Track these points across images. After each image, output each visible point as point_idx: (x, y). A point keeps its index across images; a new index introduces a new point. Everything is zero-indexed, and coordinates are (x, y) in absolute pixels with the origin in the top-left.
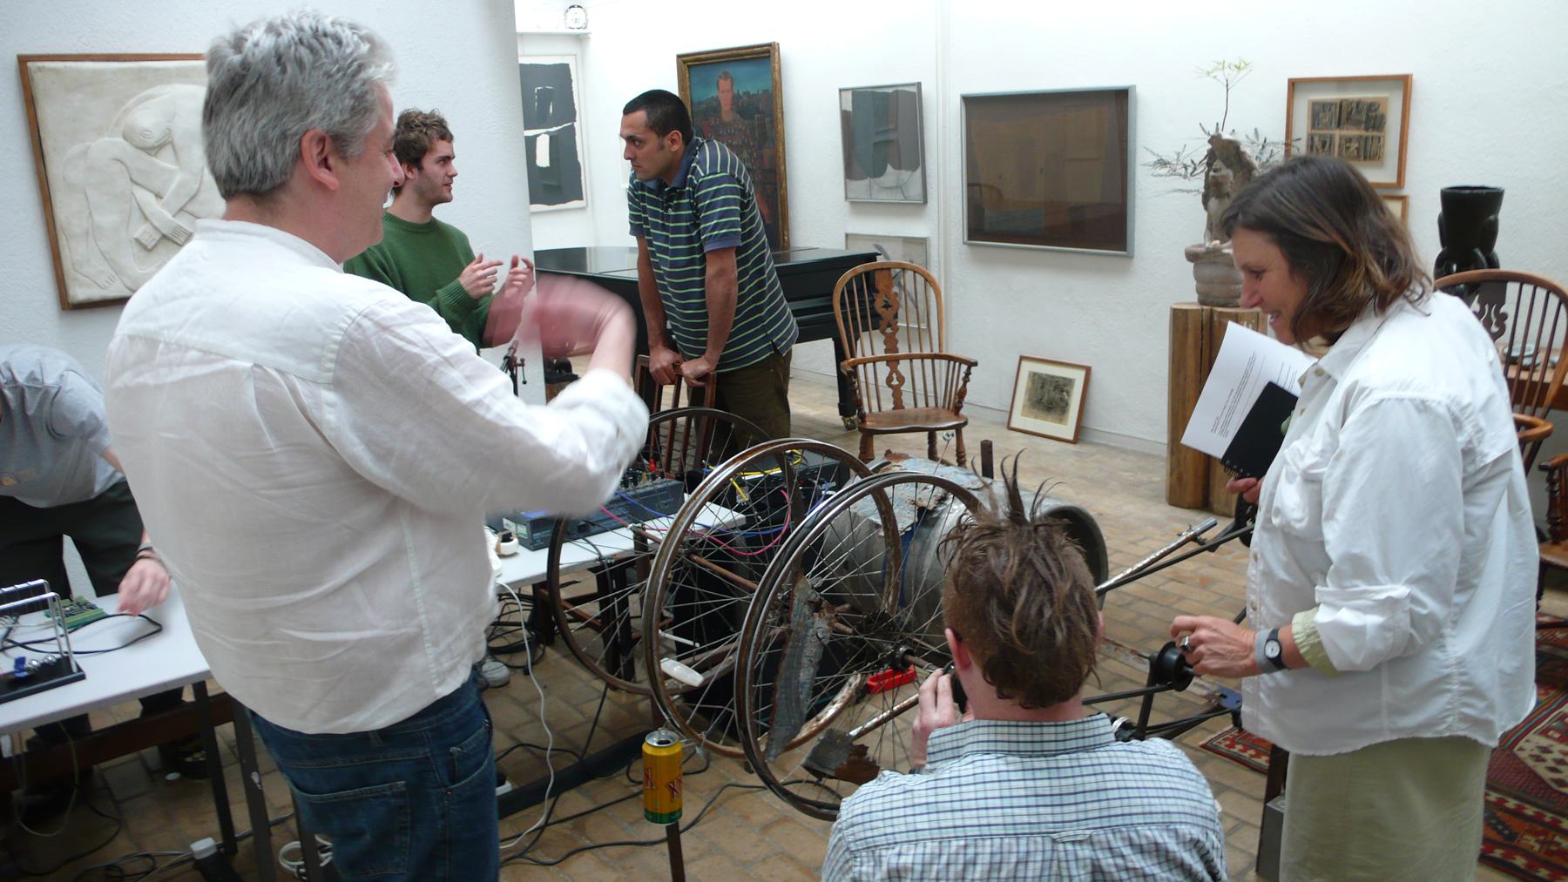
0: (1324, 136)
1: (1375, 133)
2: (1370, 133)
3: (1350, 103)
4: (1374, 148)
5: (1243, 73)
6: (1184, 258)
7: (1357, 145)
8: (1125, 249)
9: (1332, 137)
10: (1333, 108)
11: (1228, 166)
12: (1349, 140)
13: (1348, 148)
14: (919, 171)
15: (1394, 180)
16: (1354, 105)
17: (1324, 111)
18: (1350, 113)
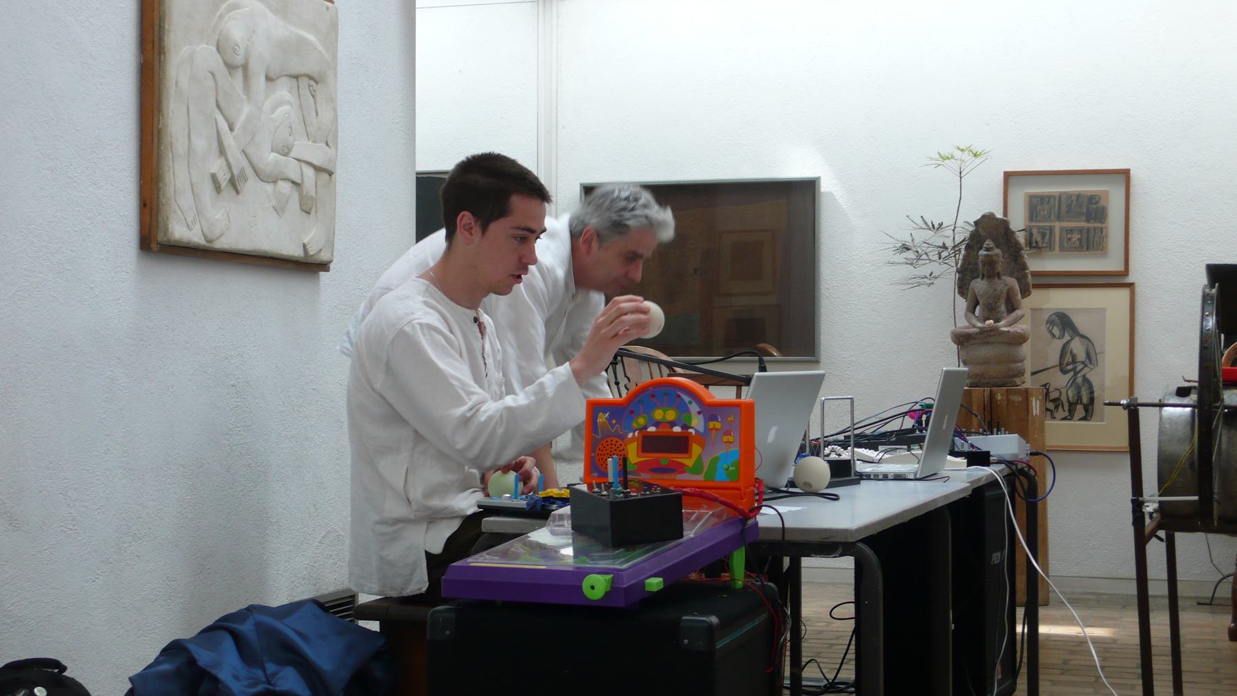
2: (1089, 225)
4: (1096, 239)
5: (978, 160)
6: (950, 340)
7: (1079, 236)
8: (814, 356)
9: (1051, 229)
10: (1052, 200)
11: (998, 246)
12: (1071, 231)
16: (1074, 198)
17: (1042, 204)
18: (1069, 206)
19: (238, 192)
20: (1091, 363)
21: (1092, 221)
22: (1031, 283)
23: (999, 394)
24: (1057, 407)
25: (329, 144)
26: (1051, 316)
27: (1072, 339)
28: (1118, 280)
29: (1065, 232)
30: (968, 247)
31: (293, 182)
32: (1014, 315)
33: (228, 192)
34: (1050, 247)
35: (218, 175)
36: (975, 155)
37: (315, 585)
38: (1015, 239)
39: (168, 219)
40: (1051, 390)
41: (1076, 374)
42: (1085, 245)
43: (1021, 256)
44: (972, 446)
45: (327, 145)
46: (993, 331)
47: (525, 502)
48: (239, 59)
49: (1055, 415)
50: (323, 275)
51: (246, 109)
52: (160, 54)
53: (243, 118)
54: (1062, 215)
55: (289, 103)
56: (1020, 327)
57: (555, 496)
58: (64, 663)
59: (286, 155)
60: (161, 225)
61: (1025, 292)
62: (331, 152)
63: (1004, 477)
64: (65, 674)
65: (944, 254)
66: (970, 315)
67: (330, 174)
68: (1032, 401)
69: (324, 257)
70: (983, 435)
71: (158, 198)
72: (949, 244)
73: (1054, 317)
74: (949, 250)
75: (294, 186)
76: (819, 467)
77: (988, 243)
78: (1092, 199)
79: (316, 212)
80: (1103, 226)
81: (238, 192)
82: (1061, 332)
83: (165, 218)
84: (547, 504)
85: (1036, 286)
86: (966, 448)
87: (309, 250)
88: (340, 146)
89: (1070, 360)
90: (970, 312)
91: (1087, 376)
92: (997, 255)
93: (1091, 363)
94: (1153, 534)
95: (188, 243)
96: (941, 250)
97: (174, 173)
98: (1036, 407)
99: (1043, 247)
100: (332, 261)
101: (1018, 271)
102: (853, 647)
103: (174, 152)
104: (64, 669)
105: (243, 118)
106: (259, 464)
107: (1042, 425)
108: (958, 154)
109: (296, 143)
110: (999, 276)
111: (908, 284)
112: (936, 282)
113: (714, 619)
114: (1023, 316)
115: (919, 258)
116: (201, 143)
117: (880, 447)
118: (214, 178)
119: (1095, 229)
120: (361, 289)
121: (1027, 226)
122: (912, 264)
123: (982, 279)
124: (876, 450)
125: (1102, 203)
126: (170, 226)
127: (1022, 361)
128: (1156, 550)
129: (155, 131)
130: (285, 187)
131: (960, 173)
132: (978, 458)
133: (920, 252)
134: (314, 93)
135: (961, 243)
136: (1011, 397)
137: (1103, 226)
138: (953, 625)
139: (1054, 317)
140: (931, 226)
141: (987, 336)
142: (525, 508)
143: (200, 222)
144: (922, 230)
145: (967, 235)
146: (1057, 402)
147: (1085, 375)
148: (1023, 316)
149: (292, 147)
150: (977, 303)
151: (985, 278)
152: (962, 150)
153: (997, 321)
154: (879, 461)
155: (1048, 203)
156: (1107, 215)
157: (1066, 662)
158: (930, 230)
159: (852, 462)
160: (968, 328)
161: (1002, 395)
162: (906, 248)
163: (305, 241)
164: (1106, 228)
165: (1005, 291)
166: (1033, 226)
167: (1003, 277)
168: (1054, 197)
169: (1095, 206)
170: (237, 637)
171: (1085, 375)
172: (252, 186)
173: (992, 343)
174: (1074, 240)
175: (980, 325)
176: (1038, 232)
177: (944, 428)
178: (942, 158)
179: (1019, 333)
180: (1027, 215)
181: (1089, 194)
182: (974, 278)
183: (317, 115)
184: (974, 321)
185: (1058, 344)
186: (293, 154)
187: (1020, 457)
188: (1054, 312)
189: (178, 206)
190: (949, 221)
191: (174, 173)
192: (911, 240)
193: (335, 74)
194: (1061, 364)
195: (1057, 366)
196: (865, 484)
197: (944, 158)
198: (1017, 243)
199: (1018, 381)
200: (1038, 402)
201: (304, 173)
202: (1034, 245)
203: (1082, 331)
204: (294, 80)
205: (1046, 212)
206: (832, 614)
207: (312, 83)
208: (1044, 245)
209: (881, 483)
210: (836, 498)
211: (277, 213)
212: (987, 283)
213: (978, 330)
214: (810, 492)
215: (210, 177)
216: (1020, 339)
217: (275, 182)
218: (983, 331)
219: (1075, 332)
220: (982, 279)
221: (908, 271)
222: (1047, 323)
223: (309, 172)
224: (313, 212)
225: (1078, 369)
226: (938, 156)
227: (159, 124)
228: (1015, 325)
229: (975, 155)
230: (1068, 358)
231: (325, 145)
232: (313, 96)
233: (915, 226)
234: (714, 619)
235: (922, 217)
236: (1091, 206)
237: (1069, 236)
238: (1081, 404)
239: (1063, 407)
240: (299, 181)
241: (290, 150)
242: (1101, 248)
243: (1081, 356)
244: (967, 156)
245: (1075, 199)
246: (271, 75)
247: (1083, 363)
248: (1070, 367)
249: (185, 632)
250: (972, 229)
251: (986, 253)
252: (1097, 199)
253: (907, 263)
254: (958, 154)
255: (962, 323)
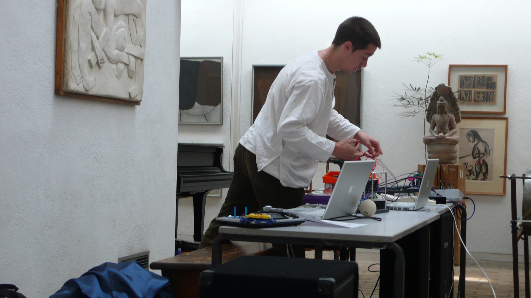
0: (466, 91)
1: (492, 90)
2: (489, 90)
3: (479, 76)
5: (437, 59)
6: (422, 142)
7: (483, 95)
9: (470, 92)
10: (471, 79)
11: (446, 99)
12: (479, 93)
13: (479, 96)
14: (219, 106)
15: (502, 111)
16: (481, 78)
17: (466, 80)
18: (479, 81)
19: (100, 68)
20: (487, 154)
21: (489, 88)
22: (461, 117)
23: (445, 168)
24: (470, 174)
25: (142, 46)
26: (469, 132)
27: (478, 143)
28: (500, 116)
29: (476, 93)
30: (432, 99)
31: (125, 64)
32: (452, 131)
33: (95, 68)
34: (470, 101)
35: (91, 60)
36: (436, 57)
37: (130, 250)
38: (454, 96)
39: (68, 80)
40: (468, 166)
41: (480, 159)
42: (486, 100)
43: (457, 104)
44: (438, 194)
45: (141, 46)
46: (443, 138)
47: (239, 220)
48: (102, 7)
49: (470, 177)
50: (137, 107)
51: (105, 30)
52: (66, 3)
53: (103, 34)
54: (475, 85)
55: (124, 27)
56: (455, 137)
57: (253, 217)
58: (17, 286)
59: (122, 51)
60: (65, 83)
61: (458, 121)
62: (142, 50)
63: (453, 209)
64: (18, 291)
65: (421, 102)
66: (432, 130)
67: (142, 60)
68: (460, 171)
69: (138, 98)
70: (442, 189)
71: (64, 70)
72: (423, 98)
73: (470, 132)
74: (423, 100)
75: (125, 66)
76: (371, 204)
77: (441, 98)
78: (490, 78)
79: (135, 77)
80: (494, 91)
81: (100, 68)
82: (473, 139)
83: (67, 80)
84: (250, 221)
85: (463, 118)
86: (435, 196)
87: (132, 95)
88: (146, 47)
89: (477, 152)
90: (432, 129)
91: (485, 160)
92: (445, 103)
93: (487, 154)
94: (520, 237)
95: (77, 92)
96: (419, 100)
97: (71, 59)
98: (461, 174)
99: (466, 100)
100: (141, 101)
101: (455, 111)
102: (379, 283)
103: (71, 49)
104: (17, 289)
105: (103, 34)
106: (106, 194)
107: (464, 183)
108: (428, 56)
109: (127, 45)
110: (446, 113)
111: (403, 115)
112: (416, 115)
113: (333, 280)
114: (456, 132)
115: (409, 103)
116: (84, 45)
117: (395, 194)
118: (89, 61)
119: (490, 92)
120: (154, 113)
121: (459, 90)
122: (405, 106)
123: (438, 114)
124: (394, 195)
125: (494, 80)
126: (69, 84)
127: (455, 152)
128: (521, 243)
129: (63, 40)
130: (121, 66)
131: (429, 65)
132: (441, 200)
133: (409, 101)
134: (135, 23)
135: (429, 97)
136: (450, 169)
137: (494, 91)
138: (430, 279)
139: (470, 132)
140: (414, 89)
141: (439, 141)
142: (239, 223)
143: (83, 82)
144: (410, 91)
145: (432, 94)
146: (471, 171)
147: (484, 159)
148: (456, 132)
149: (125, 47)
150: (435, 125)
151: (440, 114)
152: (430, 54)
153: (444, 133)
154: (396, 201)
155: (469, 80)
156: (496, 86)
157: (475, 293)
158: (414, 90)
159: (385, 202)
160: (431, 136)
161: (446, 168)
162: (403, 99)
163: (130, 91)
164: (496, 92)
165: (448, 120)
166: (462, 90)
167: (448, 114)
168: (472, 77)
169: (491, 82)
170: (100, 279)
171: (484, 159)
172: (106, 65)
173: (441, 144)
174: (481, 97)
175: (436, 135)
176: (464, 93)
177: (427, 186)
178: (421, 58)
179: (455, 140)
180: (459, 85)
181: (488, 76)
182: (434, 114)
183: (137, 32)
184: (434, 134)
185: (472, 145)
186: (126, 50)
187: (460, 200)
188: (470, 130)
189: (73, 74)
190: (423, 87)
191: (71, 59)
192: (405, 96)
193: (145, 14)
194: (473, 154)
195: (471, 155)
196: (390, 211)
197: (421, 58)
198: (455, 98)
199: (453, 161)
200: (463, 172)
201: (130, 60)
202: (462, 99)
203: (483, 139)
204: (126, 17)
205: (468, 84)
206: (369, 269)
207: (135, 18)
208: (467, 99)
209: (397, 212)
210: (380, 220)
211: (118, 78)
212: (440, 116)
213: (436, 138)
214: (367, 217)
215: (88, 61)
216: (454, 143)
217: (117, 64)
218: (438, 138)
219: (480, 139)
220: (438, 114)
221: (403, 110)
222: (467, 135)
223: (132, 59)
224: (134, 78)
225: (481, 157)
226: (419, 57)
227: (65, 36)
228: (453, 136)
229: (436, 57)
230: (476, 152)
231: (140, 47)
232: (135, 24)
233: (407, 89)
234: (333, 280)
235: (410, 85)
236: (489, 82)
237: (478, 95)
238: (482, 172)
239: (473, 174)
240: (127, 63)
241: (124, 49)
242: (493, 101)
243: (482, 150)
244: (432, 57)
245: (482, 78)
246: (117, 14)
247: (483, 154)
248: (477, 156)
249: (76, 275)
250: (434, 91)
251: (440, 102)
252: (492, 78)
253: (403, 106)
254: (428, 56)
255: (428, 134)
